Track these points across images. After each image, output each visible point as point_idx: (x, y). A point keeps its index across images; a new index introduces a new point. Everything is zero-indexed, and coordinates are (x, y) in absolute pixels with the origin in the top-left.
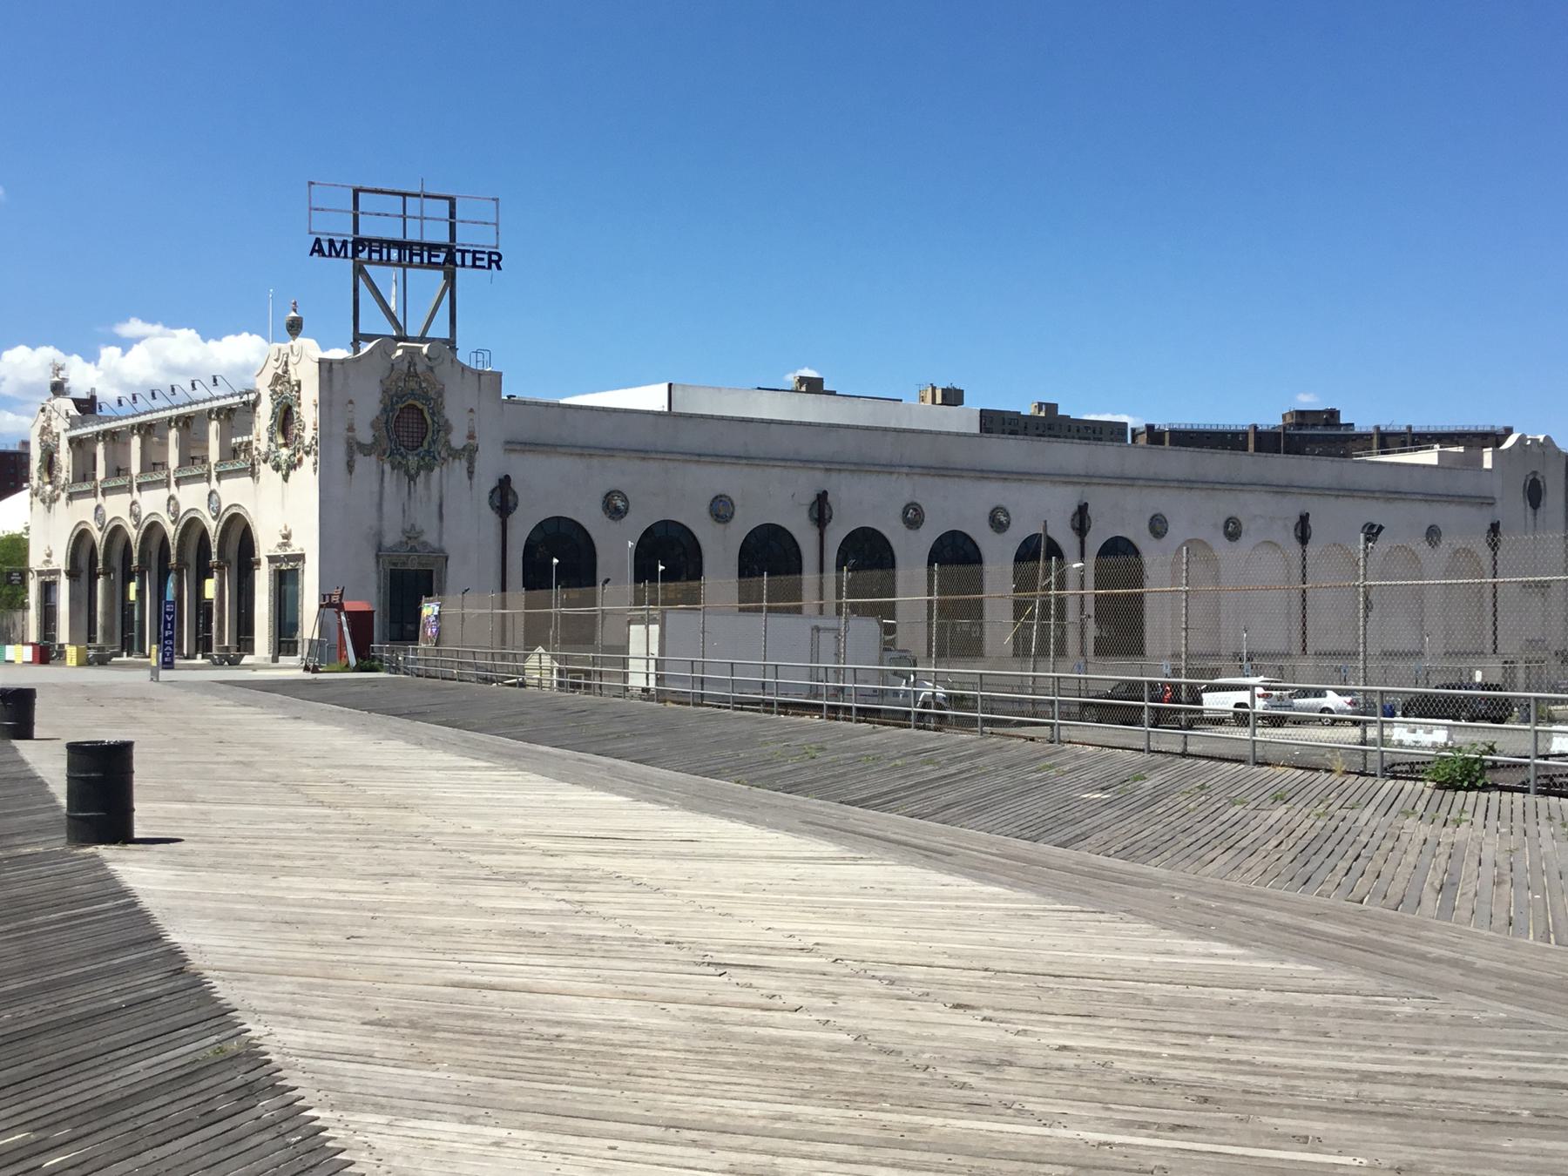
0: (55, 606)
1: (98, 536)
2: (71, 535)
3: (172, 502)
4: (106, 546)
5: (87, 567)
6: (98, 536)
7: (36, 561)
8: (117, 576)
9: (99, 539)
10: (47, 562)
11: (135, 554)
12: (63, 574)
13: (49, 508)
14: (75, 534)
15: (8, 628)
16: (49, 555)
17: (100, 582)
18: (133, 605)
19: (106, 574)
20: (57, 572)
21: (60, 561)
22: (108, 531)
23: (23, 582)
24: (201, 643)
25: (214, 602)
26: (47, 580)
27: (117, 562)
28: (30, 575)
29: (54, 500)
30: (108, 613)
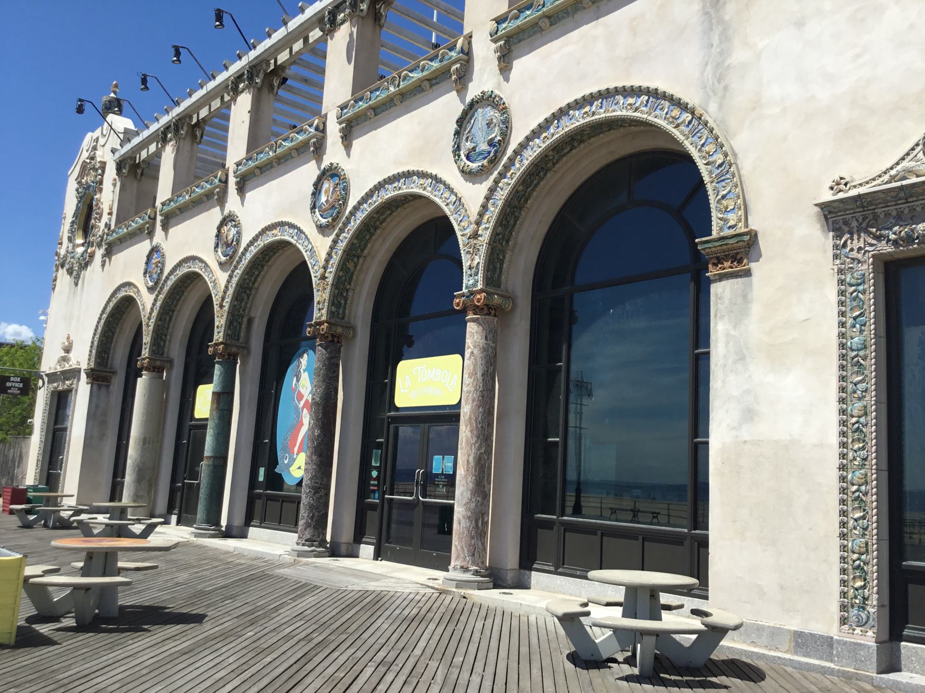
0: (65, 429)
1: (147, 302)
2: (103, 312)
3: (327, 185)
4: (160, 317)
5: (125, 365)
6: (147, 302)
7: (49, 363)
8: (175, 376)
9: (149, 307)
10: (65, 359)
11: (220, 321)
12: (83, 376)
13: (77, 278)
14: (109, 309)
15: (13, 461)
16: (67, 350)
17: (142, 384)
18: (204, 427)
19: (156, 369)
20: (74, 374)
21: (82, 357)
22: (166, 289)
23: (28, 387)
24: (373, 518)
25: (466, 411)
26: (60, 388)
27: (176, 350)
28: (40, 383)
29: (85, 263)
30: (151, 442)
